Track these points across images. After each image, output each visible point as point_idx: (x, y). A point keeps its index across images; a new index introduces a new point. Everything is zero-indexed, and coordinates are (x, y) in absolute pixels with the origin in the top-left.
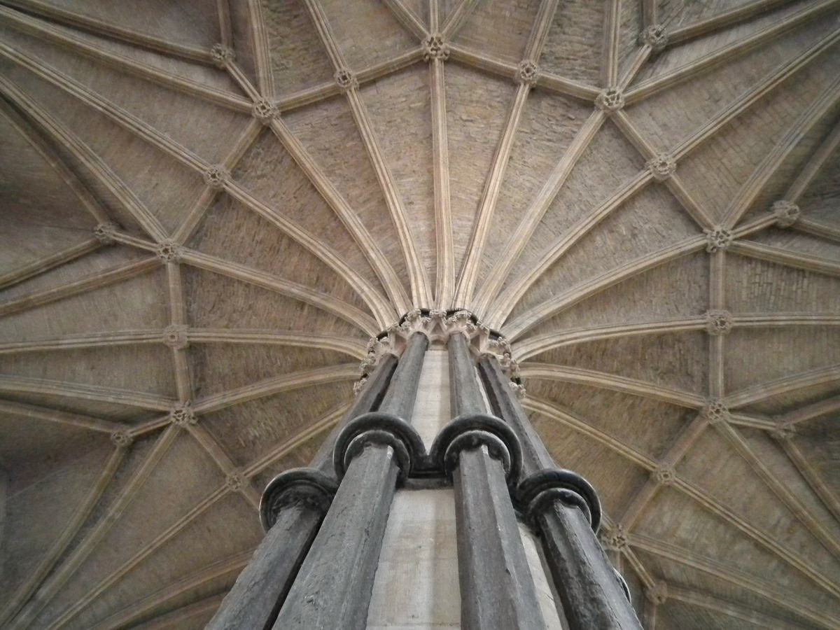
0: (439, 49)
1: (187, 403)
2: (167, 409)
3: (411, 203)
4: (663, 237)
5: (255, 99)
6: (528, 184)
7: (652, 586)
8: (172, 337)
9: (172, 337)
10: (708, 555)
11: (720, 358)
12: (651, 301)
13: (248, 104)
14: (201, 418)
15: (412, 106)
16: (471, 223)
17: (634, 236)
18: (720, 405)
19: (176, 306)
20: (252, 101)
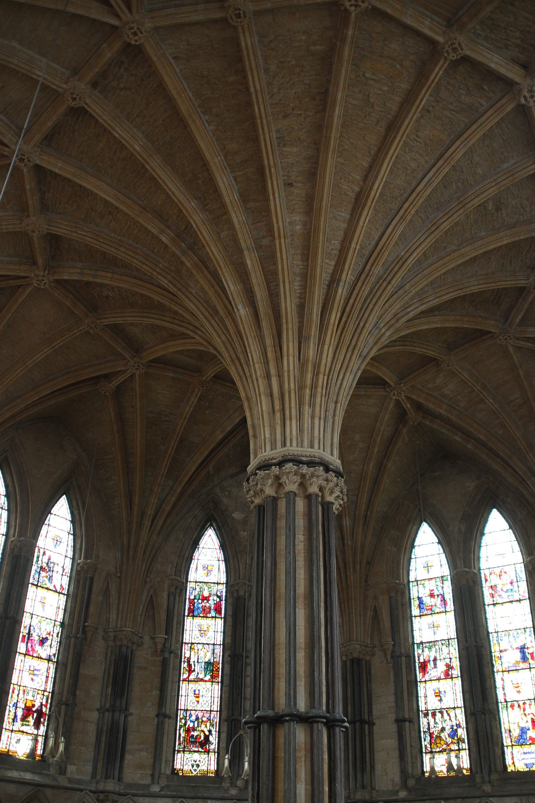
0: (360, 6)
1: (47, 272)
2: (28, 275)
3: (291, 185)
4: (525, 211)
5: (122, 15)
6: (413, 165)
7: (411, 414)
8: (33, 231)
9: (33, 231)
10: (458, 406)
11: (526, 306)
12: (490, 258)
13: (114, 22)
14: (57, 281)
15: (312, 48)
16: (345, 225)
17: (498, 209)
18: (509, 336)
19: (33, 201)
20: (118, 16)
